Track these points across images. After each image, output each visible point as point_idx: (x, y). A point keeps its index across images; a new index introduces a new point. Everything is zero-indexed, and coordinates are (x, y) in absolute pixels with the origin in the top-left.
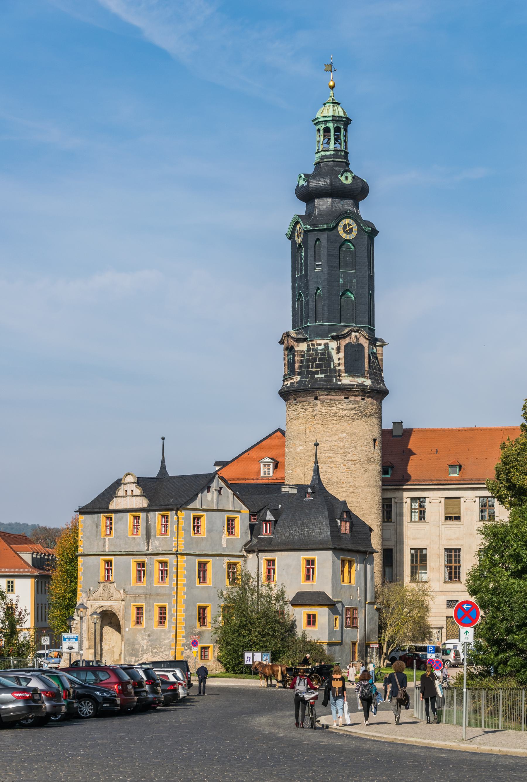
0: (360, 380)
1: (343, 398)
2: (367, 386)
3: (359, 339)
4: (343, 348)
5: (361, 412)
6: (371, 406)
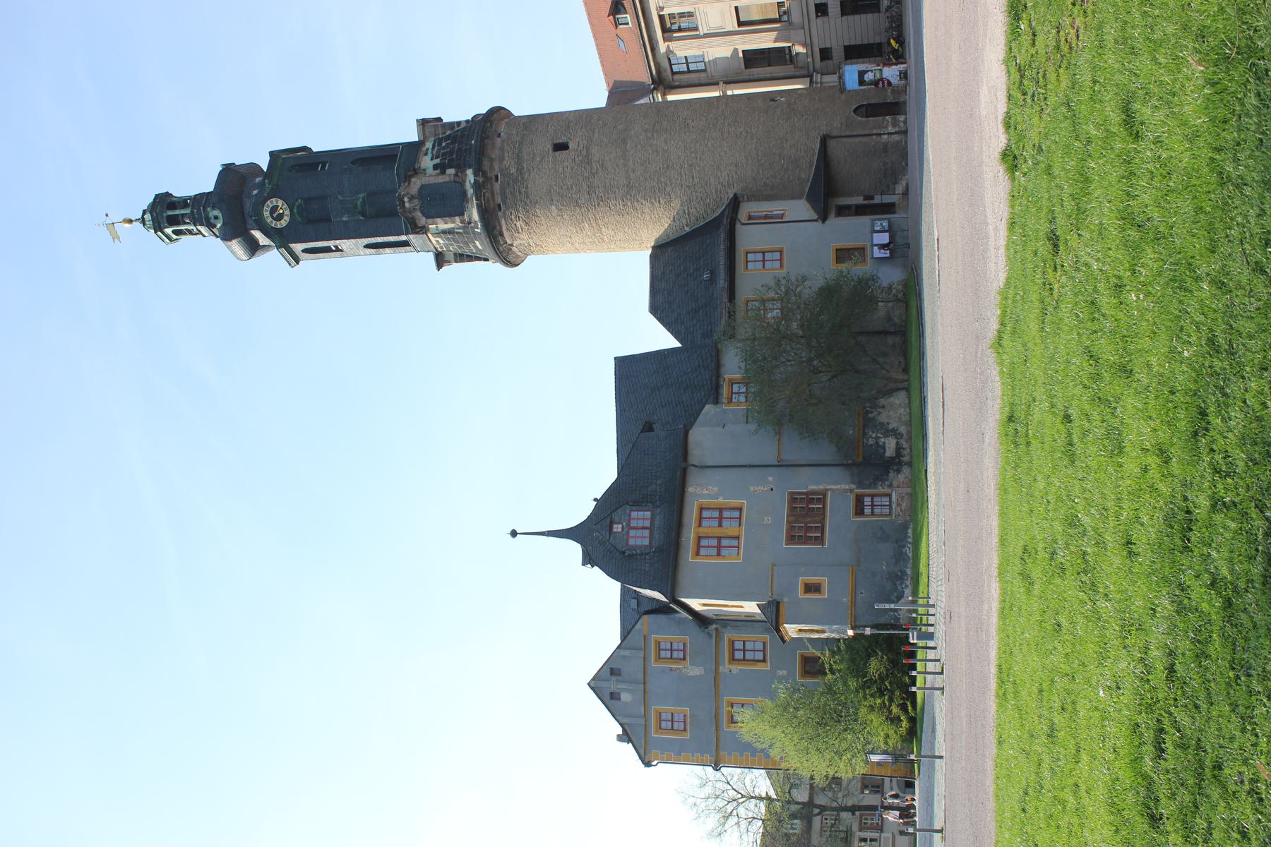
1: (500, 214)
2: (475, 180)
3: (412, 196)
4: (430, 221)
6: (505, 162)
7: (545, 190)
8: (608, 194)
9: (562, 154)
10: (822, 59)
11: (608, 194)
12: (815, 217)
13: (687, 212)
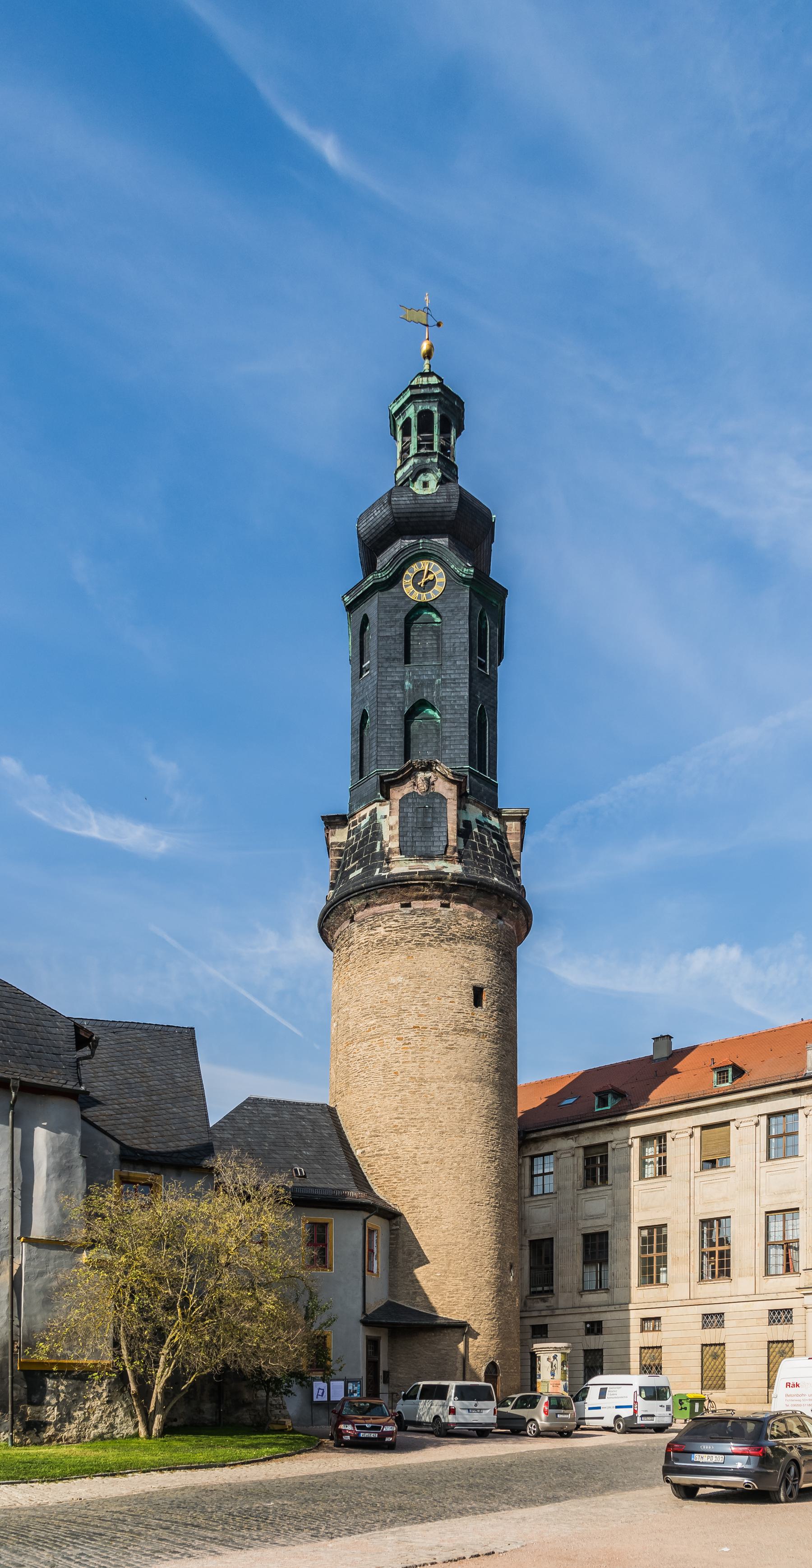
0: (432, 866)
1: (397, 906)
5: (441, 931)
6: (466, 919)
7: (424, 969)
8: (413, 1053)
9: (468, 998)
10: (534, 1327)
11: (413, 1053)
12: (368, 1313)
13: (382, 1152)
